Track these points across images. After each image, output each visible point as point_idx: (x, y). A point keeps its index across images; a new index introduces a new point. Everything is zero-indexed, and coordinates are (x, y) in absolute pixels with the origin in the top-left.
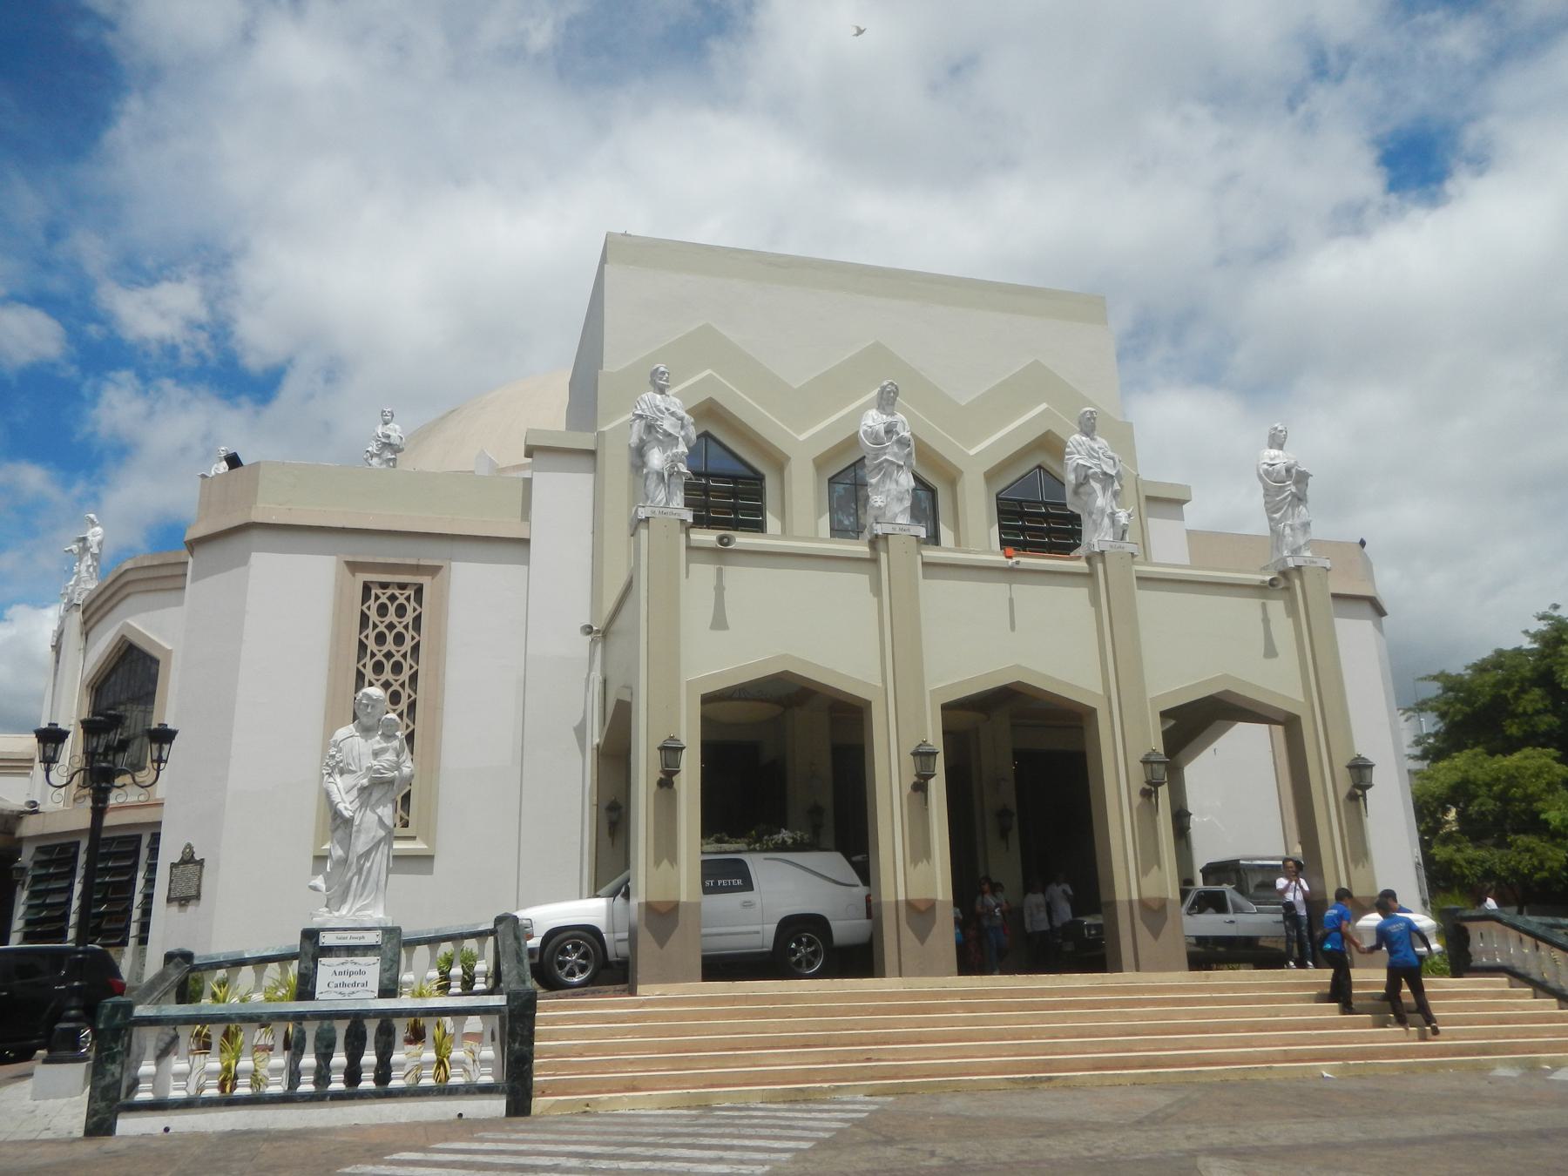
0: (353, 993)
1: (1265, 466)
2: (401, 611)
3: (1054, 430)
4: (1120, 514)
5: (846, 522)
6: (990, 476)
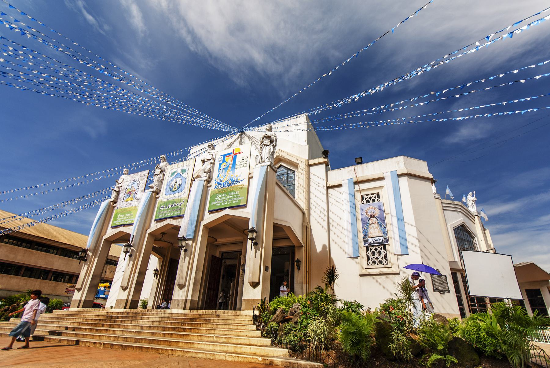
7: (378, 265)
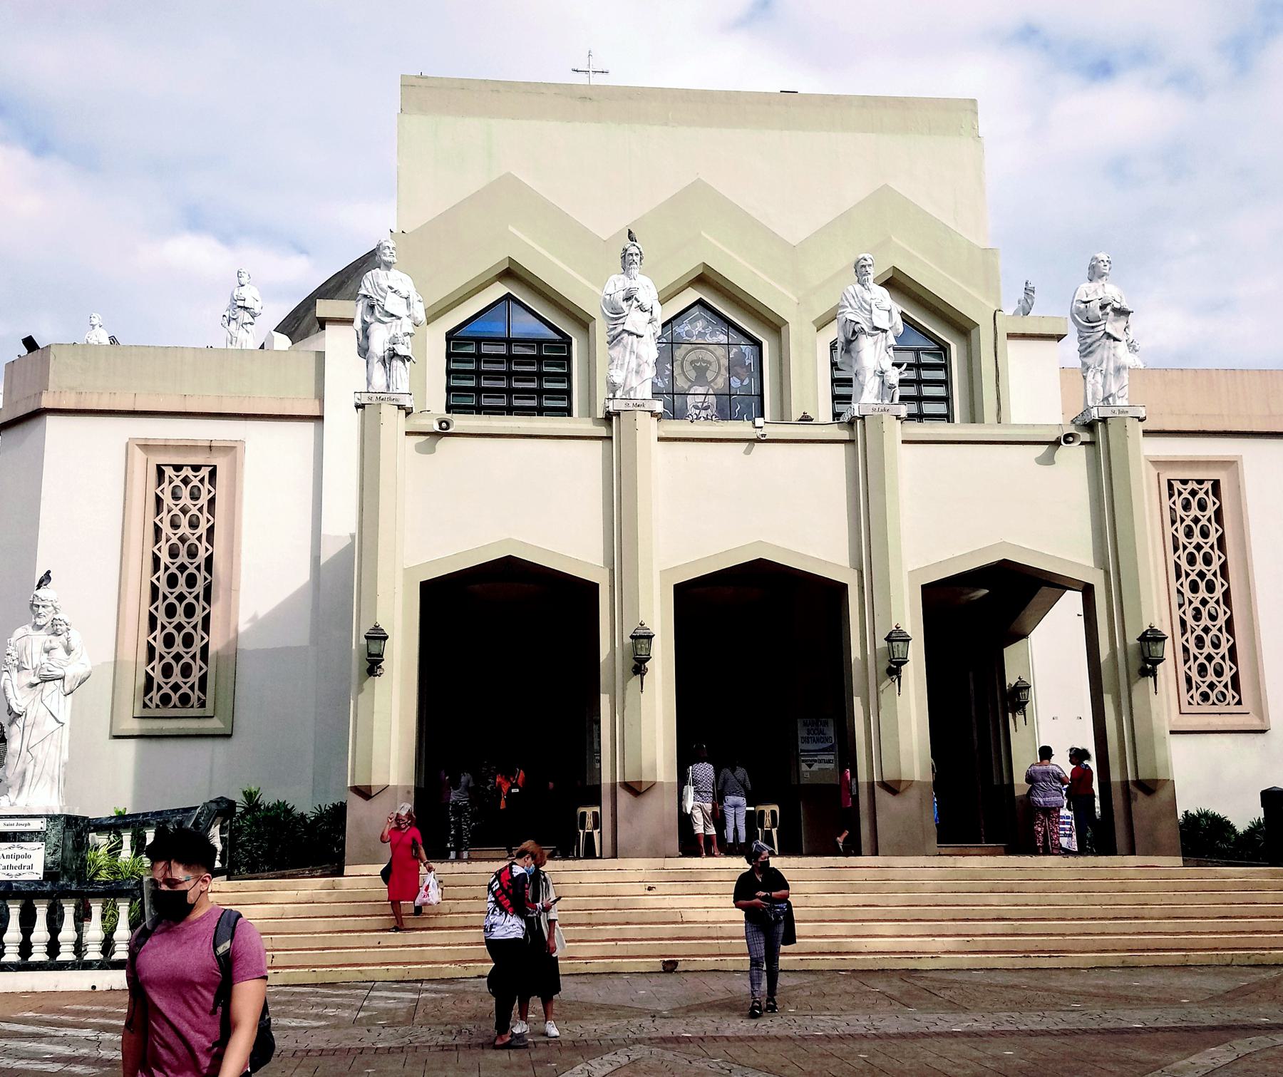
0: (20, 874)
7: (175, 706)
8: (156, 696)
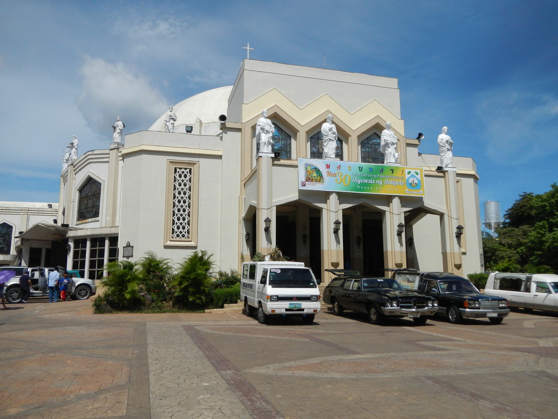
1: (440, 140)
2: (185, 176)
3: (379, 123)
4: (396, 155)
5: (315, 151)
6: (359, 137)
7: (181, 238)
8: (175, 235)
